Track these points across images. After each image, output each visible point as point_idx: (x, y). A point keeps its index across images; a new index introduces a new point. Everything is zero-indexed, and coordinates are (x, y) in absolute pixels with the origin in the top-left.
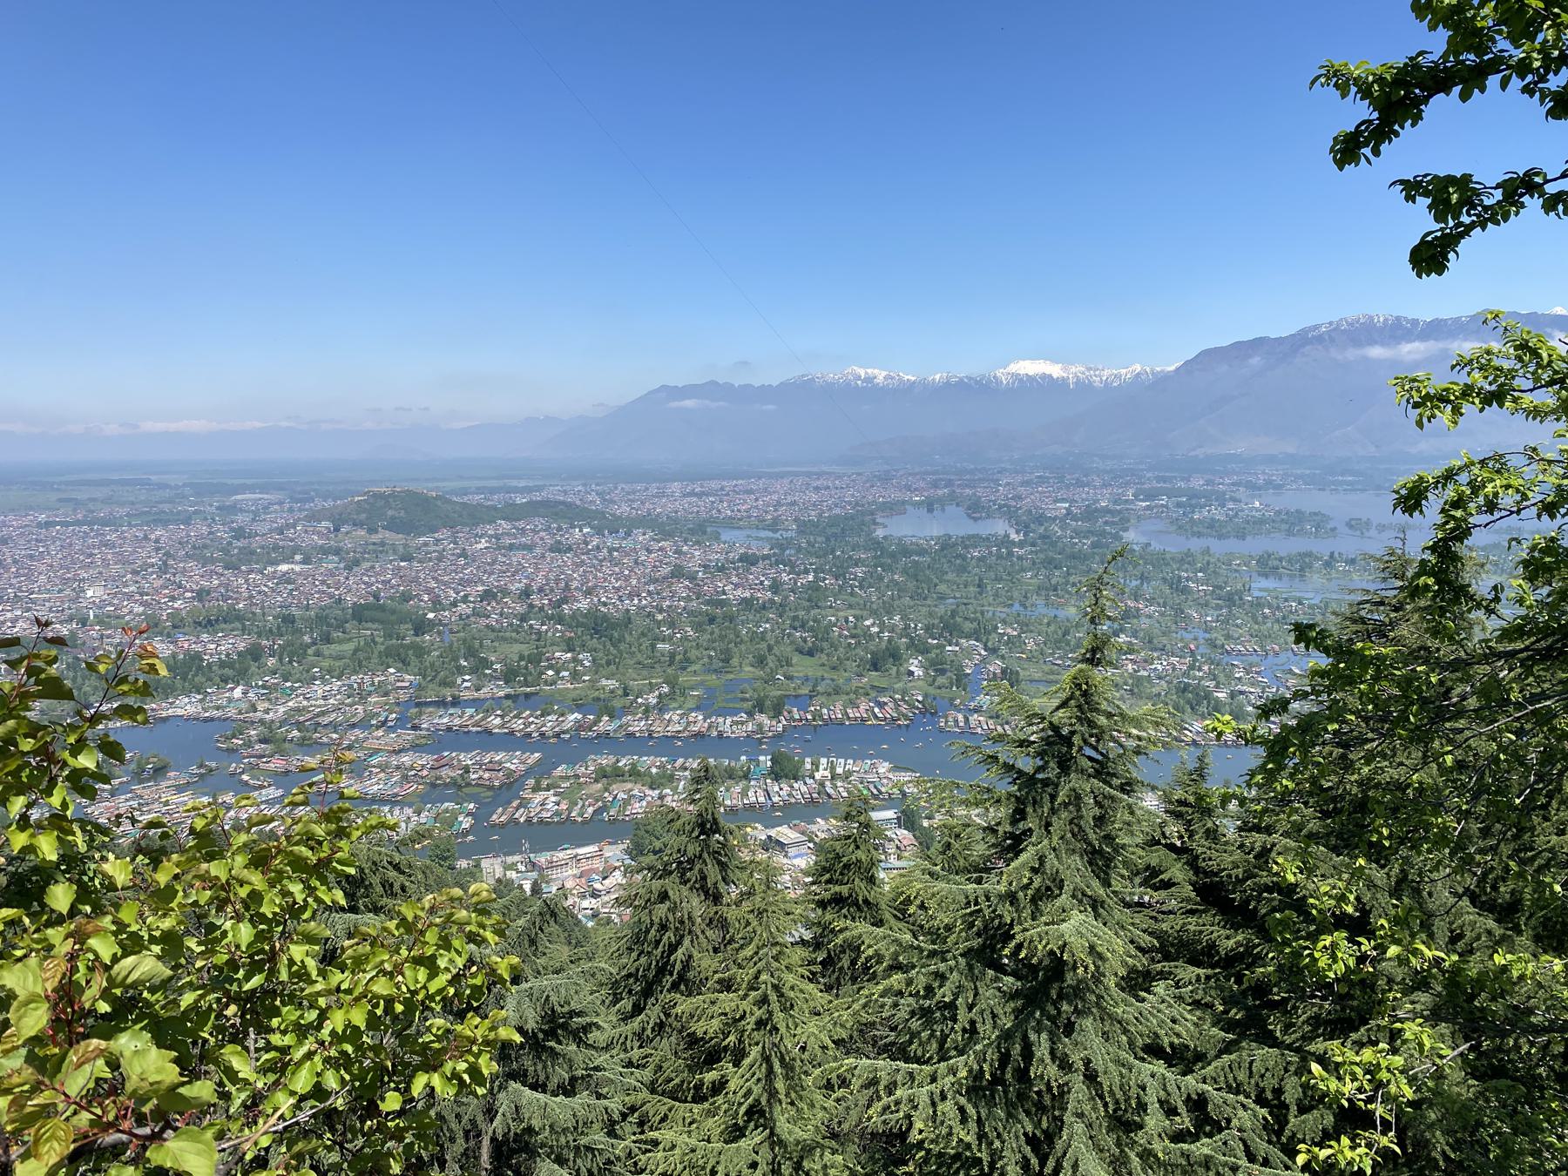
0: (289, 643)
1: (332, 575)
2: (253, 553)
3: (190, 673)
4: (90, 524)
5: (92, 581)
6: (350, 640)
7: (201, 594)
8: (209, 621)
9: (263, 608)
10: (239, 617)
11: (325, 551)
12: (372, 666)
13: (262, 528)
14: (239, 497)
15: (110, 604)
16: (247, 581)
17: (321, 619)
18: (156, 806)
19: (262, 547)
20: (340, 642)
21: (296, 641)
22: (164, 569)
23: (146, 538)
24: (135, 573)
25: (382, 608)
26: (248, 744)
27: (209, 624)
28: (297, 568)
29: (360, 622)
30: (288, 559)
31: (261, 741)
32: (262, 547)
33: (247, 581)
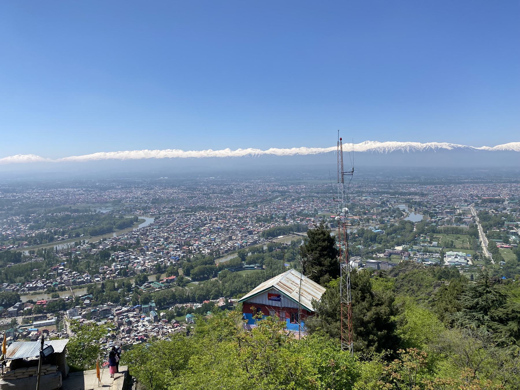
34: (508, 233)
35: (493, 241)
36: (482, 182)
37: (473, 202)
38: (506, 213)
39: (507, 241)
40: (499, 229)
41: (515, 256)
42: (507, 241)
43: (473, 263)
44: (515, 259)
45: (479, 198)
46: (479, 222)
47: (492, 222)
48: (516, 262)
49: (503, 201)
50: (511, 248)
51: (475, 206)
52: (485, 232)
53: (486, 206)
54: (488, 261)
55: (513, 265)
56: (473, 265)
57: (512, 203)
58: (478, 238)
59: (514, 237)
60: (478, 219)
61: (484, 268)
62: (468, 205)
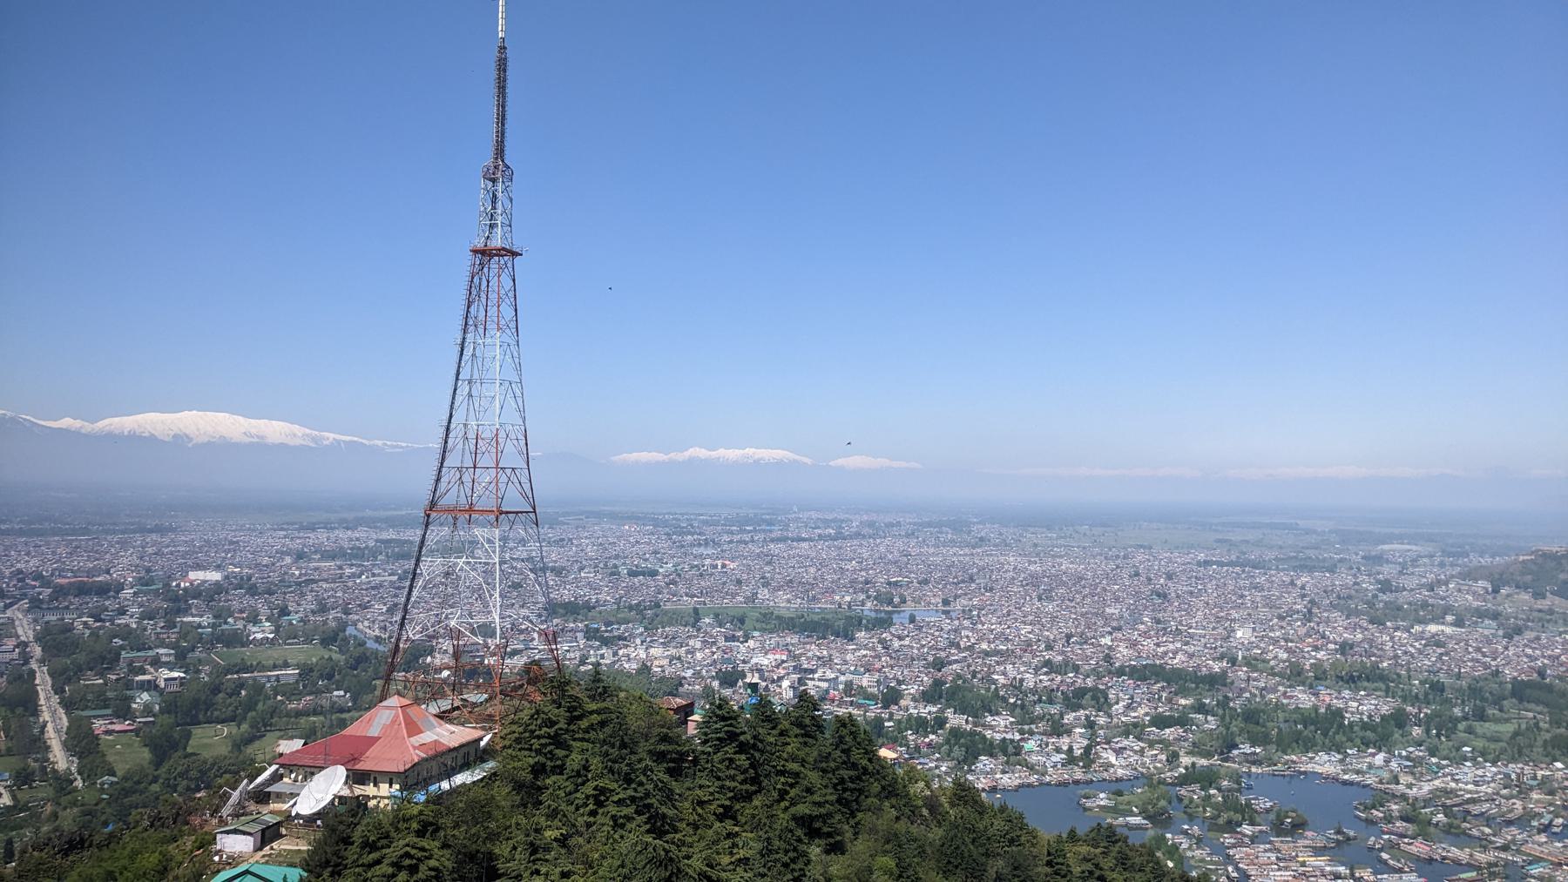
0: (1436, 714)
1: (1489, 642)
2: (1399, 608)
3: (1327, 730)
4: (1242, 565)
5: (1243, 622)
6: (1507, 720)
7: (1345, 647)
8: (1352, 677)
9: (1409, 670)
10: (1383, 677)
11: (1481, 614)
12: (1534, 756)
13: (1410, 582)
14: (1386, 547)
15: (1258, 647)
16: (1392, 638)
17: (1474, 691)
18: (1294, 866)
19: (1410, 604)
20: (1497, 721)
21: (1449, 712)
22: (1309, 616)
23: (1292, 583)
24: (1281, 618)
25: (1550, 688)
26: (1389, 819)
27: (1352, 680)
28: (1448, 630)
29: (1521, 700)
30: (1438, 619)
31: (1403, 819)
32: (1410, 604)
33: (1392, 638)
34: (129, 685)
35: (82, 718)
36: (54, 533)
37: (24, 596)
38: (127, 625)
39: (124, 712)
40: (101, 675)
41: (146, 754)
42: (123, 711)
43: (14, 797)
44: (145, 764)
45: (46, 583)
46: (42, 661)
47: (81, 657)
48: (150, 770)
49: (120, 587)
50: (137, 732)
51: (29, 610)
52: (58, 690)
53: (67, 608)
54: (62, 783)
55: (139, 782)
56: (14, 807)
57: (145, 593)
58: (36, 712)
59: (145, 696)
60: (37, 651)
61: (49, 808)
62: (7, 607)
